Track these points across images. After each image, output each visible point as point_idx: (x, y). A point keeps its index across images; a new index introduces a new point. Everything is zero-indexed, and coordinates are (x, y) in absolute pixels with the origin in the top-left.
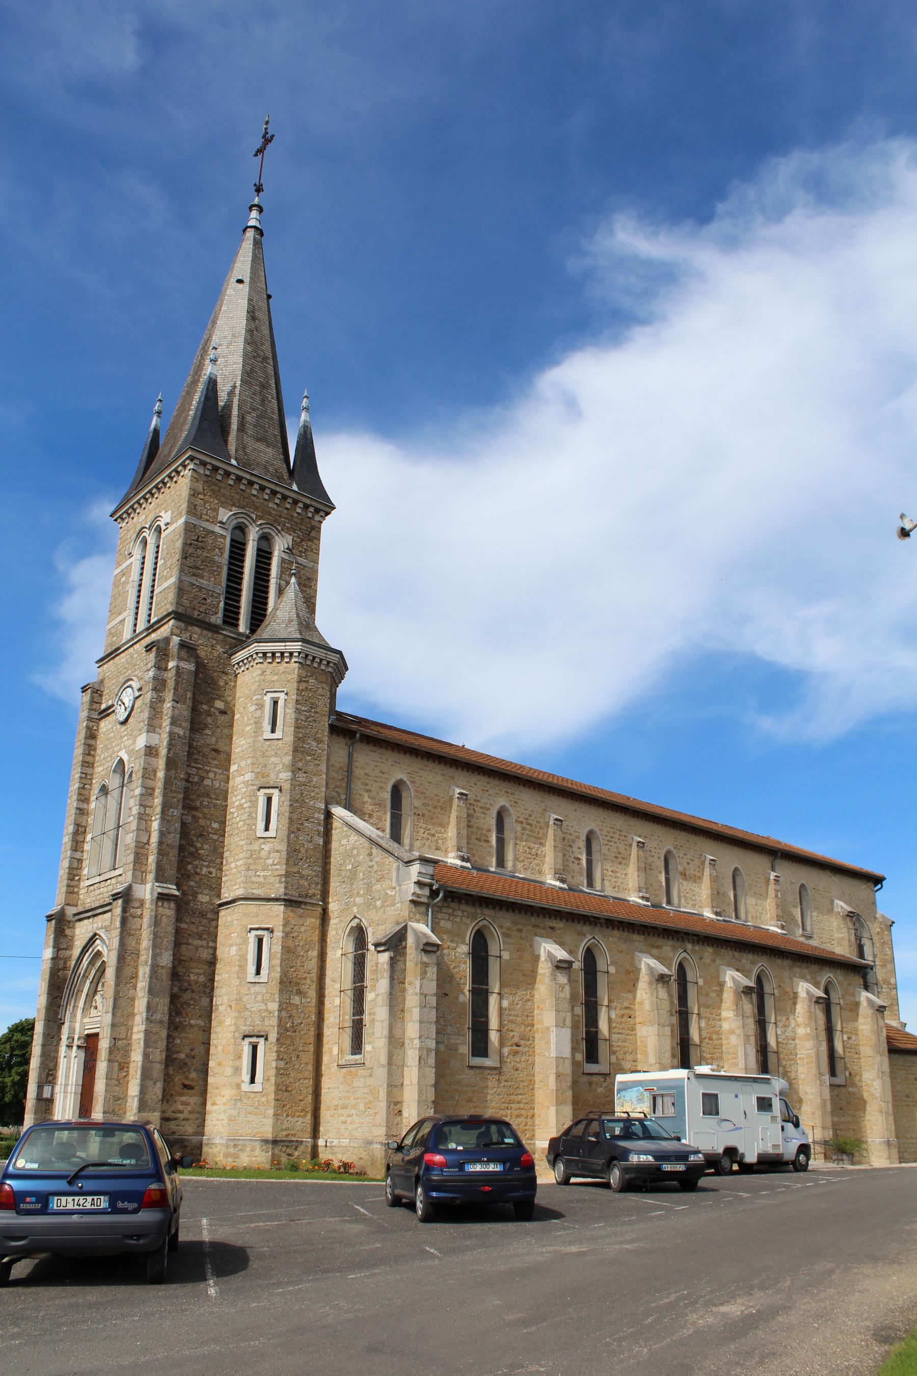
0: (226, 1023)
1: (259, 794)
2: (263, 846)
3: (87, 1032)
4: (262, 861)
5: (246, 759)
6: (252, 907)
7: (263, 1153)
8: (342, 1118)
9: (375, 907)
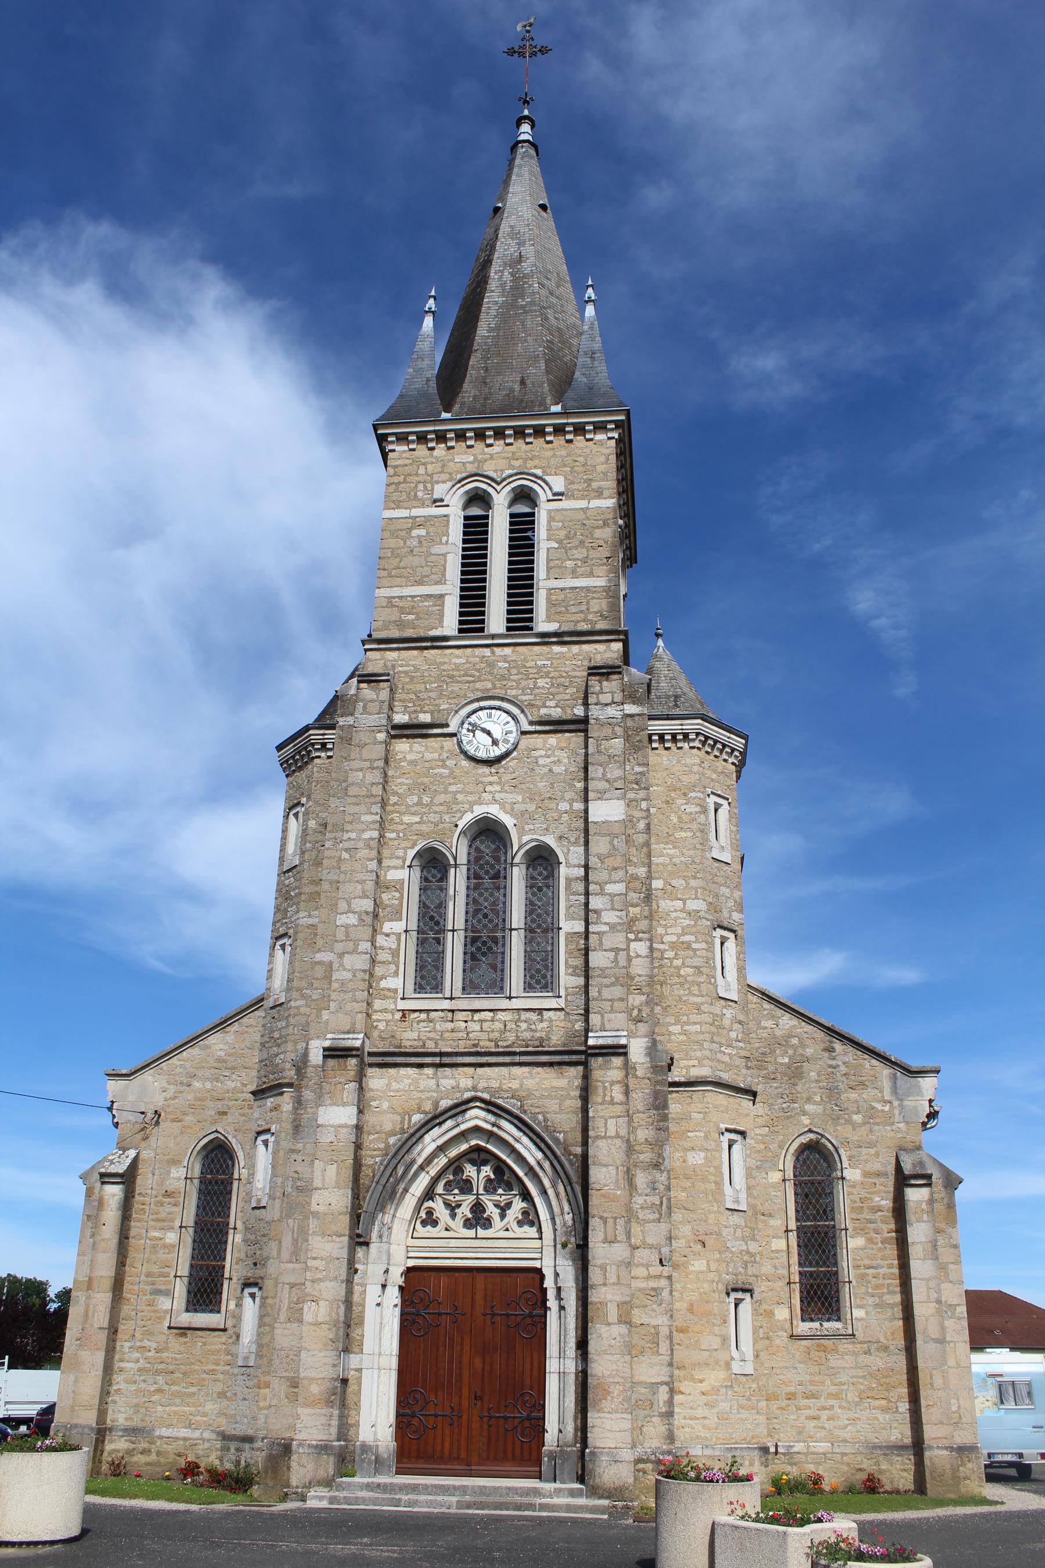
0: (691, 1268)
1: (714, 934)
3: (411, 1263)
4: (725, 1032)
5: (684, 878)
6: (719, 1098)
7: (763, 1468)
8: (808, 1412)
9: (849, 1121)
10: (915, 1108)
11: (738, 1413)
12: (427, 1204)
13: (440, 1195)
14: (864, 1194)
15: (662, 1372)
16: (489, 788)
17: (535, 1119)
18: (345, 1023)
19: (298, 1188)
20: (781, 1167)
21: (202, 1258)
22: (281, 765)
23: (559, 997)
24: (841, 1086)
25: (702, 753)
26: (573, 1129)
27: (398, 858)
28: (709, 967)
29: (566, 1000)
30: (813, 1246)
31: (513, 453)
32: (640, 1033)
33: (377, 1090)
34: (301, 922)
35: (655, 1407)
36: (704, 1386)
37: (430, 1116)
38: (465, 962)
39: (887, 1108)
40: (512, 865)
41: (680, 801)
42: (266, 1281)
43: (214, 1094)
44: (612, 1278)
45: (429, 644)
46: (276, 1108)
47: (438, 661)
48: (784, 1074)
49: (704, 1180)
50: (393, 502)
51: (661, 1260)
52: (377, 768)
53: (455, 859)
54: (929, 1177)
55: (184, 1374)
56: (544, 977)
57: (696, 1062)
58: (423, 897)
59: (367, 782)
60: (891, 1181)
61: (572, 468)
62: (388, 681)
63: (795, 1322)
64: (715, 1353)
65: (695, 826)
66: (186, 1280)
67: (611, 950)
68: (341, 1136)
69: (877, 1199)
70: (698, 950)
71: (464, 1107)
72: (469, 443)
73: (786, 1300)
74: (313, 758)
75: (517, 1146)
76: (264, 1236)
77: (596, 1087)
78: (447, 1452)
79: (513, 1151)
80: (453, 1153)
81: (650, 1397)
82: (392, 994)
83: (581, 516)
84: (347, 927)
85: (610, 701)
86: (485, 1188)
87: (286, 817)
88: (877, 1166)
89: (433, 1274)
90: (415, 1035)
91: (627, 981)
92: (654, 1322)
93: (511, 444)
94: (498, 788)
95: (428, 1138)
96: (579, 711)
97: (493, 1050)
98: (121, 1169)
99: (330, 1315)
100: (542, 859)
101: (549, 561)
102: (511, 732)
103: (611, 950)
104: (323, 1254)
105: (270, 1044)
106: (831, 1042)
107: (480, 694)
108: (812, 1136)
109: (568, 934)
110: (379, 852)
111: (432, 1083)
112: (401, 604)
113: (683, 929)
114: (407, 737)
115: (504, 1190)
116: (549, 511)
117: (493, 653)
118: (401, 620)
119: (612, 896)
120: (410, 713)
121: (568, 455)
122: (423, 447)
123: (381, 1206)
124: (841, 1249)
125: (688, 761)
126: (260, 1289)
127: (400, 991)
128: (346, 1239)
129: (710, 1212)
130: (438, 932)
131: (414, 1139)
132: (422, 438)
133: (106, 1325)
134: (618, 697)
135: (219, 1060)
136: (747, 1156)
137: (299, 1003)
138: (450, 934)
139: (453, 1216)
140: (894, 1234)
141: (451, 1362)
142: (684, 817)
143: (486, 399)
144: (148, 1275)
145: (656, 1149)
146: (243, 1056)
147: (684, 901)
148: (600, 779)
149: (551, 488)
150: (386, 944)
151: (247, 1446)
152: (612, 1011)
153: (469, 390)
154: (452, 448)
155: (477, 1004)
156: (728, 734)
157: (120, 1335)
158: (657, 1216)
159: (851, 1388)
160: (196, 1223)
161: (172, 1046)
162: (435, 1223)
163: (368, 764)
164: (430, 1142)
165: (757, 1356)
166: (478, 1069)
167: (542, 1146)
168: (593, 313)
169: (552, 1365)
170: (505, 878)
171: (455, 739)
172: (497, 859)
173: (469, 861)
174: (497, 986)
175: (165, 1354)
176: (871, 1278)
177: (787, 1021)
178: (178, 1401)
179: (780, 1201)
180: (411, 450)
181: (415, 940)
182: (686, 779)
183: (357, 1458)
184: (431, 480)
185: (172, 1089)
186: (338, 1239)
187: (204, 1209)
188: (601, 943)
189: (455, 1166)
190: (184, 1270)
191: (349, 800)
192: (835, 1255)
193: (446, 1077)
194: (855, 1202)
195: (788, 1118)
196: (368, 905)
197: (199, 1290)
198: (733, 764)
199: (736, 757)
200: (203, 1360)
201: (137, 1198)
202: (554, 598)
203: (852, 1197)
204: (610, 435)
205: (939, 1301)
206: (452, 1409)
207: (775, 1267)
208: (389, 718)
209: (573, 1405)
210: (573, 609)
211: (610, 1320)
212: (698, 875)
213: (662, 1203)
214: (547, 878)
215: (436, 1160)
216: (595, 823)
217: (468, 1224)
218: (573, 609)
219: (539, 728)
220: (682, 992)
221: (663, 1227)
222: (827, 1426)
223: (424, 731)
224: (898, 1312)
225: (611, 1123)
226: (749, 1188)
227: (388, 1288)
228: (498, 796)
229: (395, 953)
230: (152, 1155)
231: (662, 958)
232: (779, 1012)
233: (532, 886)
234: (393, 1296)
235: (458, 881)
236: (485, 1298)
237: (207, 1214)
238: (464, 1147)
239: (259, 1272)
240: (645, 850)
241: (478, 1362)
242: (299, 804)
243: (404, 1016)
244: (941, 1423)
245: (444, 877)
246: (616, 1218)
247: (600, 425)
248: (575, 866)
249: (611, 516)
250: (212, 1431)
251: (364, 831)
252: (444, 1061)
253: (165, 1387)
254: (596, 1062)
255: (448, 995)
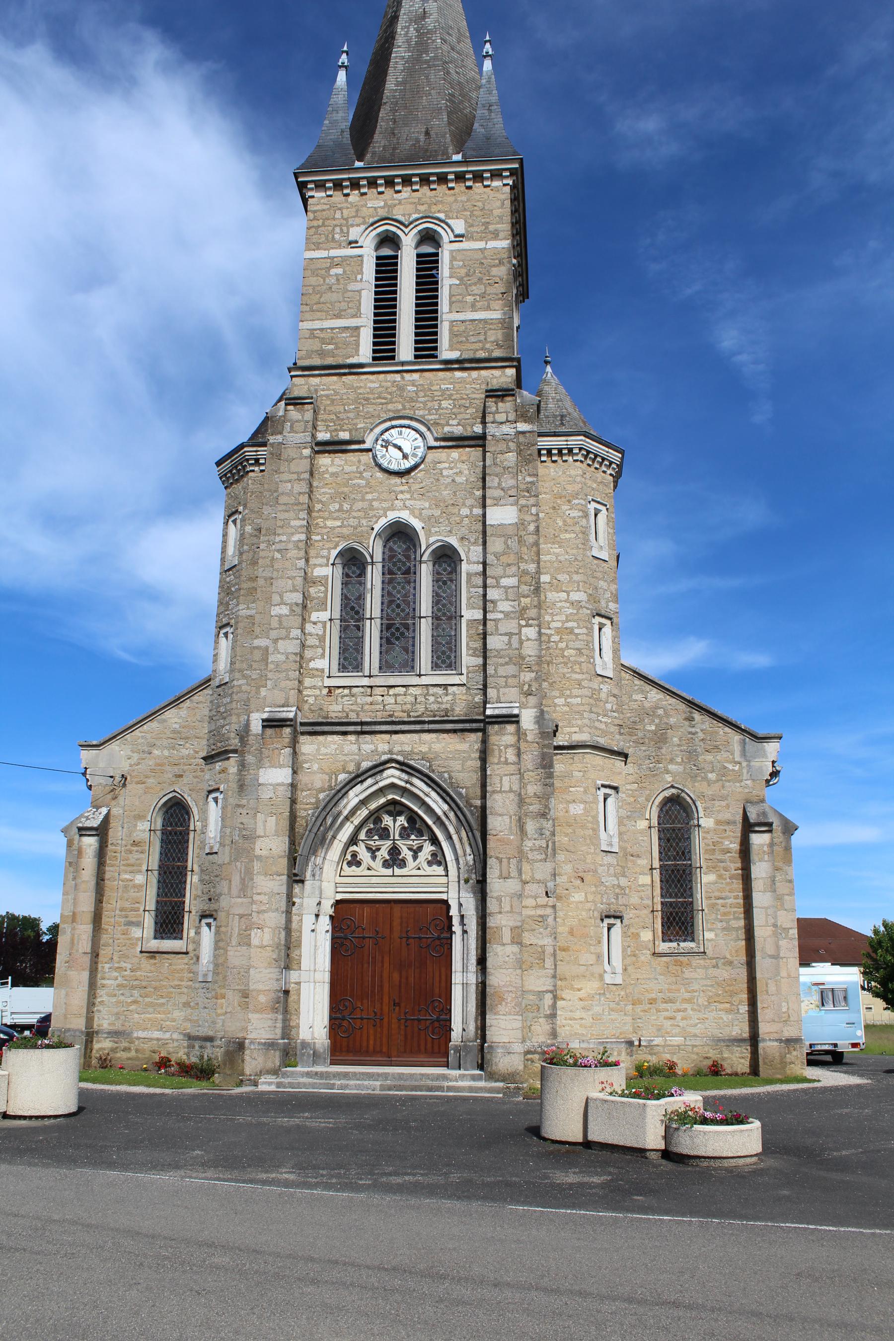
0: (572, 899)
1: (594, 621)
2: (602, 686)
3: (339, 897)
4: (602, 704)
5: (568, 573)
7: (628, 1057)
9: (705, 778)
10: (761, 767)
11: (609, 1015)
12: (352, 848)
13: (362, 841)
14: (716, 839)
15: (547, 983)
16: (400, 496)
17: (441, 777)
18: (280, 698)
19: (244, 836)
20: (647, 817)
21: (166, 895)
22: (221, 478)
23: (462, 674)
24: (699, 750)
25: (584, 466)
26: (474, 785)
27: (322, 557)
28: (589, 649)
29: (468, 677)
30: (673, 881)
31: (419, 199)
32: (530, 705)
33: (309, 754)
34: (241, 613)
35: (541, 1010)
36: (582, 994)
37: (353, 775)
38: (381, 645)
39: (737, 768)
40: (421, 562)
41: (565, 507)
42: (219, 913)
43: (172, 760)
44: (507, 908)
45: (347, 371)
46: (223, 771)
47: (355, 385)
48: (651, 739)
49: (583, 827)
50: (313, 243)
51: (547, 893)
52: (304, 479)
53: (372, 557)
54: (770, 825)
55: (155, 988)
56: (449, 657)
57: (577, 729)
58: (345, 591)
59: (295, 492)
60: (738, 828)
61: (472, 212)
62: (311, 403)
63: (657, 943)
64: (591, 968)
65: (577, 528)
66: (153, 913)
67: (506, 634)
68: (279, 793)
69: (727, 843)
70: (579, 634)
71: (381, 768)
72: (380, 189)
73: (650, 925)
74: (248, 472)
75: (427, 799)
76: (217, 876)
77: (493, 750)
78: (371, 1048)
79: (424, 804)
80: (373, 806)
81: (537, 1002)
82: (320, 673)
83: (479, 255)
84: (280, 616)
85: (504, 419)
86: (400, 835)
87: (226, 523)
88: (727, 816)
89: (358, 905)
90: (340, 708)
91: (519, 660)
92: (541, 943)
93: (417, 191)
94: (408, 496)
95: (351, 794)
96: (478, 429)
97: (406, 719)
98: (95, 823)
99: (273, 940)
100: (446, 557)
101: (451, 296)
102: (419, 447)
103: (506, 634)
104: (266, 890)
105: (217, 718)
106: (691, 713)
107: (392, 415)
108: (674, 791)
109: (468, 621)
110: (306, 552)
111: (355, 747)
112: (322, 336)
113: (567, 616)
114: (329, 452)
115: (416, 836)
116: (451, 252)
117: (403, 378)
118: (323, 350)
119: (506, 588)
120: (331, 432)
121: (468, 200)
122: (339, 193)
123: (313, 851)
124: (696, 883)
125: (573, 472)
126: (215, 919)
127: (327, 671)
128: (285, 878)
129: (588, 853)
130: (358, 620)
131: (340, 795)
132: (338, 185)
133: (89, 950)
134: (512, 417)
135: (174, 731)
136: (620, 807)
137: (240, 682)
138: (368, 622)
139: (374, 858)
140: (740, 872)
141: (373, 976)
142: (568, 520)
143: (394, 149)
144: (121, 910)
145: (543, 801)
146: (194, 728)
147: (568, 593)
148: (496, 488)
149: (452, 231)
150: (313, 631)
151: (208, 1044)
152: (506, 686)
153: (379, 141)
154: (365, 194)
155: (392, 681)
156: (607, 449)
157: (101, 959)
158: (544, 856)
159: (702, 994)
160: (160, 867)
161: (135, 721)
162: (358, 864)
163: (295, 476)
164: (354, 797)
165: (625, 970)
166: (393, 736)
167: (448, 799)
168: (490, 68)
169: (457, 978)
170: (415, 573)
171: (370, 453)
172: (408, 558)
173: (383, 559)
174: (409, 665)
175: (139, 973)
176: (720, 907)
177: (654, 695)
178: (151, 1010)
179: (647, 844)
180: (328, 196)
181: (338, 627)
182: (570, 488)
183: (298, 1053)
184: (346, 224)
185: (136, 756)
186: (278, 878)
187: (166, 855)
188: (497, 629)
189: (375, 817)
190: (151, 905)
191: (280, 508)
192: (691, 888)
193: (367, 743)
194: (709, 845)
195: (654, 776)
196: (297, 597)
197: (164, 921)
198: (611, 475)
199: (614, 469)
200: (170, 977)
201: (110, 847)
202: (456, 329)
203: (706, 841)
204: (505, 182)
205: (775, 925)
206: (376, 1013)
207: (642, 898)
208: (313, 436)
209: (474, 1010)
210: (472, 339)
211: (505, 942)
212: (580, 571)
213: (548, 846)
214: (451, 573)
215: (359, 812)
216: (491, 526)
217: (386, 864)
218: (472, 339)
219: (443, 444)
220: (566, 670)
221: (549, 866)
222: (681, 1024)
223: (344, 447)
224: (742, 934)
225: (506, 779)
226: (620, 834)
227: (321, 918)
228: (408, 503)
229: (322, 639)
230: (121, 812)
231: (549, 642)
232: (648, 688)
233: (438, 580)
234: (325, 923)
235: (374, 577)
236: (401, 924)
237: (169, 859)
238: (382, 801)
239: (213, 906)
240: (534, 549)
241: (396, 976)
242: (236, 512)
243: (330, 692)
244: (774, 1021)
245: (363, 573)
246: (509, 858)
247: (496, 172)
248: (474, 563)
249: (506, 256)
250: (180, 1033)
251: (293, 534)
252: (364, 729)
253: (140, 999)
254: (493, 729)
255: (367, 673)
